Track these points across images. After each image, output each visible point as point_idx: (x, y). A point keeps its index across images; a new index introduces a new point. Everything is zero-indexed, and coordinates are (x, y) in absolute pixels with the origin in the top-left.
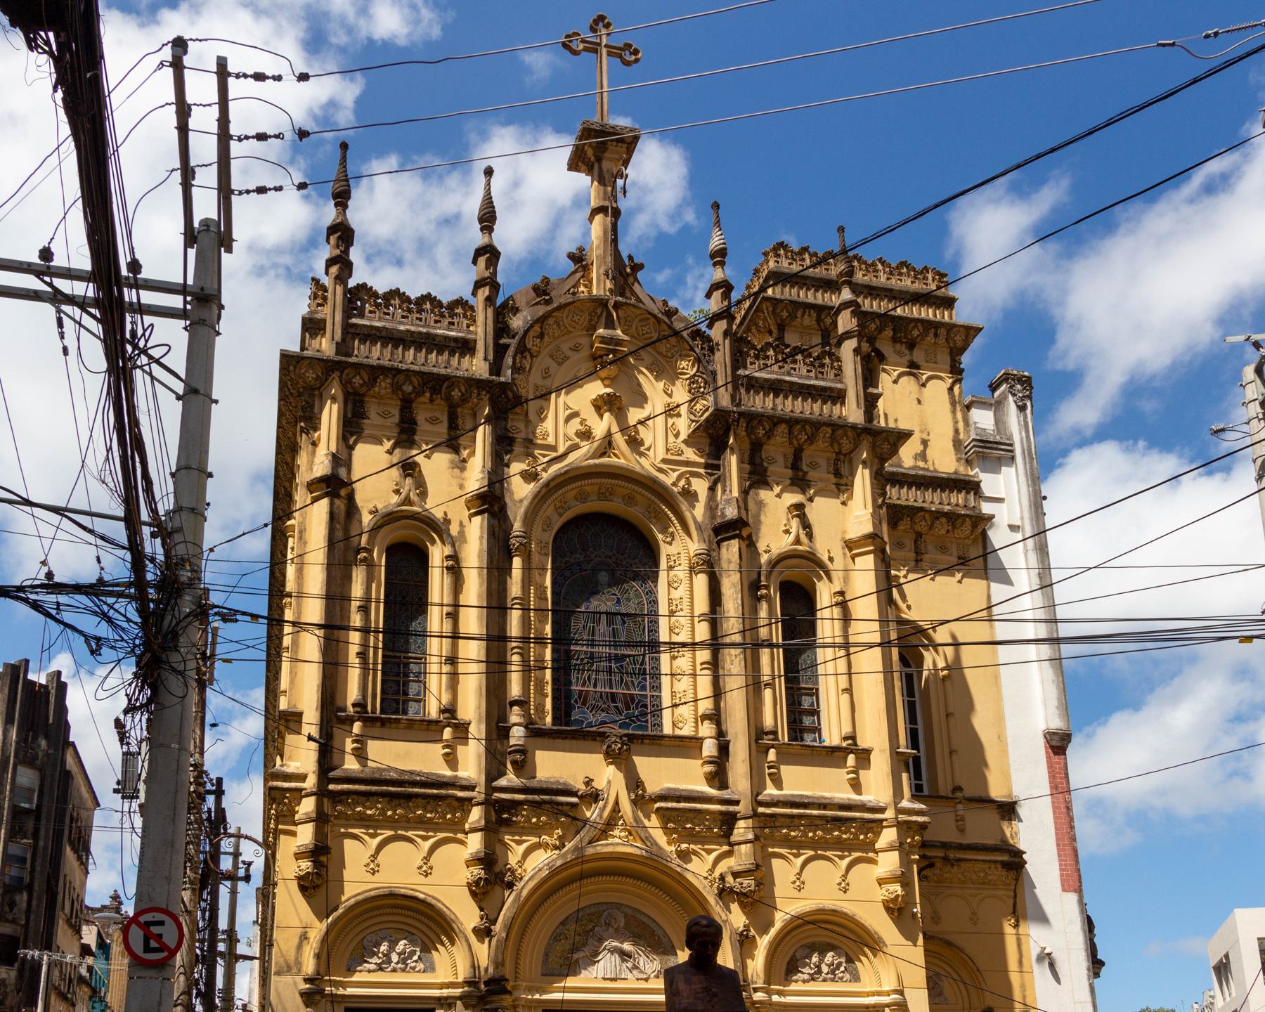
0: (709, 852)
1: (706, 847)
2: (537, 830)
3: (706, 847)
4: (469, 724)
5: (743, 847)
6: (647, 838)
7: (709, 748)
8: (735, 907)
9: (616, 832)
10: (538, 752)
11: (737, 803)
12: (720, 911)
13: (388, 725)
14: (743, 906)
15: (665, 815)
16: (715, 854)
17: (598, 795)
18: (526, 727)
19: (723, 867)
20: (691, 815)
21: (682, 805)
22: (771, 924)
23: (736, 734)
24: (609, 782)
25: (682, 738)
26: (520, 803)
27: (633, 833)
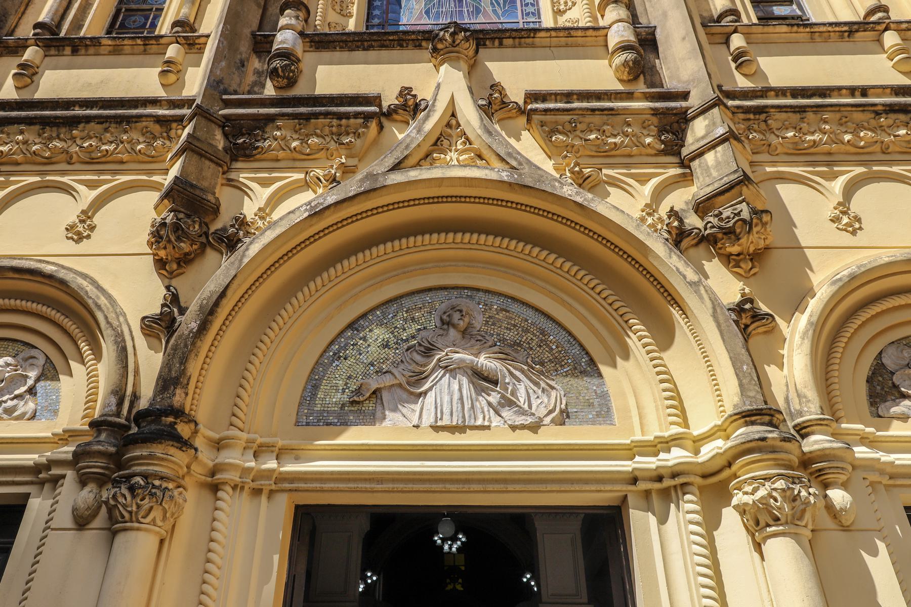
0: (643, 180)
1: (633, 171)
2: (299, 159)
3: (633, 171)
4: (208, 36)
5: (710, 157)
6: (509, 154)
7: (619, 34)
8: (714, 268)
9: (453, 155)
10: (320, 68)
11: (685, 96)
12: (681, 265)
13: (83, 52)
14: (730, 261)
15: (548, 133)
16: (654, 181)
17: (417, 105)
18: (302, 34)
19: (680, 198)
20: (597, 119)
21: (576, 105)
22: (810, 292)
23: (665, 14)
24: (438, 86)
25: (568, 31)
26: (271, 119)
27: (486, 153)
